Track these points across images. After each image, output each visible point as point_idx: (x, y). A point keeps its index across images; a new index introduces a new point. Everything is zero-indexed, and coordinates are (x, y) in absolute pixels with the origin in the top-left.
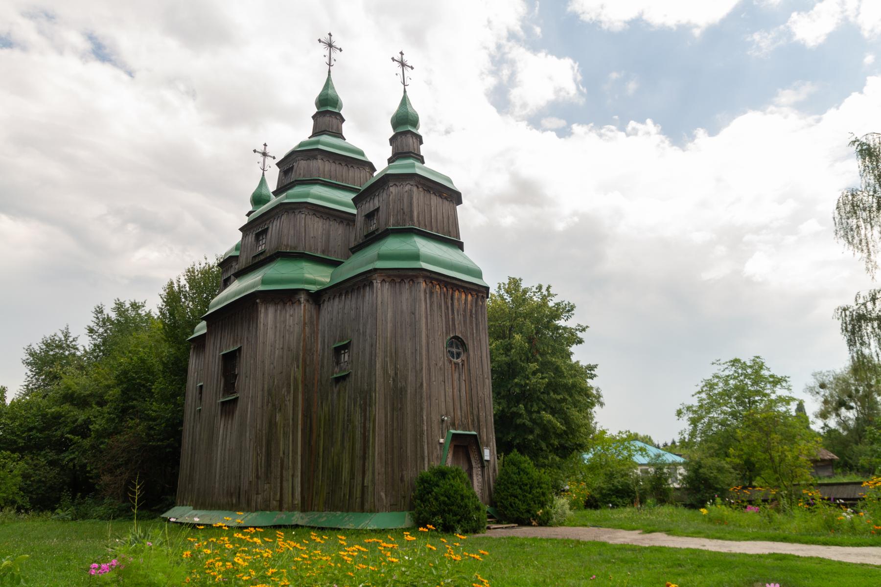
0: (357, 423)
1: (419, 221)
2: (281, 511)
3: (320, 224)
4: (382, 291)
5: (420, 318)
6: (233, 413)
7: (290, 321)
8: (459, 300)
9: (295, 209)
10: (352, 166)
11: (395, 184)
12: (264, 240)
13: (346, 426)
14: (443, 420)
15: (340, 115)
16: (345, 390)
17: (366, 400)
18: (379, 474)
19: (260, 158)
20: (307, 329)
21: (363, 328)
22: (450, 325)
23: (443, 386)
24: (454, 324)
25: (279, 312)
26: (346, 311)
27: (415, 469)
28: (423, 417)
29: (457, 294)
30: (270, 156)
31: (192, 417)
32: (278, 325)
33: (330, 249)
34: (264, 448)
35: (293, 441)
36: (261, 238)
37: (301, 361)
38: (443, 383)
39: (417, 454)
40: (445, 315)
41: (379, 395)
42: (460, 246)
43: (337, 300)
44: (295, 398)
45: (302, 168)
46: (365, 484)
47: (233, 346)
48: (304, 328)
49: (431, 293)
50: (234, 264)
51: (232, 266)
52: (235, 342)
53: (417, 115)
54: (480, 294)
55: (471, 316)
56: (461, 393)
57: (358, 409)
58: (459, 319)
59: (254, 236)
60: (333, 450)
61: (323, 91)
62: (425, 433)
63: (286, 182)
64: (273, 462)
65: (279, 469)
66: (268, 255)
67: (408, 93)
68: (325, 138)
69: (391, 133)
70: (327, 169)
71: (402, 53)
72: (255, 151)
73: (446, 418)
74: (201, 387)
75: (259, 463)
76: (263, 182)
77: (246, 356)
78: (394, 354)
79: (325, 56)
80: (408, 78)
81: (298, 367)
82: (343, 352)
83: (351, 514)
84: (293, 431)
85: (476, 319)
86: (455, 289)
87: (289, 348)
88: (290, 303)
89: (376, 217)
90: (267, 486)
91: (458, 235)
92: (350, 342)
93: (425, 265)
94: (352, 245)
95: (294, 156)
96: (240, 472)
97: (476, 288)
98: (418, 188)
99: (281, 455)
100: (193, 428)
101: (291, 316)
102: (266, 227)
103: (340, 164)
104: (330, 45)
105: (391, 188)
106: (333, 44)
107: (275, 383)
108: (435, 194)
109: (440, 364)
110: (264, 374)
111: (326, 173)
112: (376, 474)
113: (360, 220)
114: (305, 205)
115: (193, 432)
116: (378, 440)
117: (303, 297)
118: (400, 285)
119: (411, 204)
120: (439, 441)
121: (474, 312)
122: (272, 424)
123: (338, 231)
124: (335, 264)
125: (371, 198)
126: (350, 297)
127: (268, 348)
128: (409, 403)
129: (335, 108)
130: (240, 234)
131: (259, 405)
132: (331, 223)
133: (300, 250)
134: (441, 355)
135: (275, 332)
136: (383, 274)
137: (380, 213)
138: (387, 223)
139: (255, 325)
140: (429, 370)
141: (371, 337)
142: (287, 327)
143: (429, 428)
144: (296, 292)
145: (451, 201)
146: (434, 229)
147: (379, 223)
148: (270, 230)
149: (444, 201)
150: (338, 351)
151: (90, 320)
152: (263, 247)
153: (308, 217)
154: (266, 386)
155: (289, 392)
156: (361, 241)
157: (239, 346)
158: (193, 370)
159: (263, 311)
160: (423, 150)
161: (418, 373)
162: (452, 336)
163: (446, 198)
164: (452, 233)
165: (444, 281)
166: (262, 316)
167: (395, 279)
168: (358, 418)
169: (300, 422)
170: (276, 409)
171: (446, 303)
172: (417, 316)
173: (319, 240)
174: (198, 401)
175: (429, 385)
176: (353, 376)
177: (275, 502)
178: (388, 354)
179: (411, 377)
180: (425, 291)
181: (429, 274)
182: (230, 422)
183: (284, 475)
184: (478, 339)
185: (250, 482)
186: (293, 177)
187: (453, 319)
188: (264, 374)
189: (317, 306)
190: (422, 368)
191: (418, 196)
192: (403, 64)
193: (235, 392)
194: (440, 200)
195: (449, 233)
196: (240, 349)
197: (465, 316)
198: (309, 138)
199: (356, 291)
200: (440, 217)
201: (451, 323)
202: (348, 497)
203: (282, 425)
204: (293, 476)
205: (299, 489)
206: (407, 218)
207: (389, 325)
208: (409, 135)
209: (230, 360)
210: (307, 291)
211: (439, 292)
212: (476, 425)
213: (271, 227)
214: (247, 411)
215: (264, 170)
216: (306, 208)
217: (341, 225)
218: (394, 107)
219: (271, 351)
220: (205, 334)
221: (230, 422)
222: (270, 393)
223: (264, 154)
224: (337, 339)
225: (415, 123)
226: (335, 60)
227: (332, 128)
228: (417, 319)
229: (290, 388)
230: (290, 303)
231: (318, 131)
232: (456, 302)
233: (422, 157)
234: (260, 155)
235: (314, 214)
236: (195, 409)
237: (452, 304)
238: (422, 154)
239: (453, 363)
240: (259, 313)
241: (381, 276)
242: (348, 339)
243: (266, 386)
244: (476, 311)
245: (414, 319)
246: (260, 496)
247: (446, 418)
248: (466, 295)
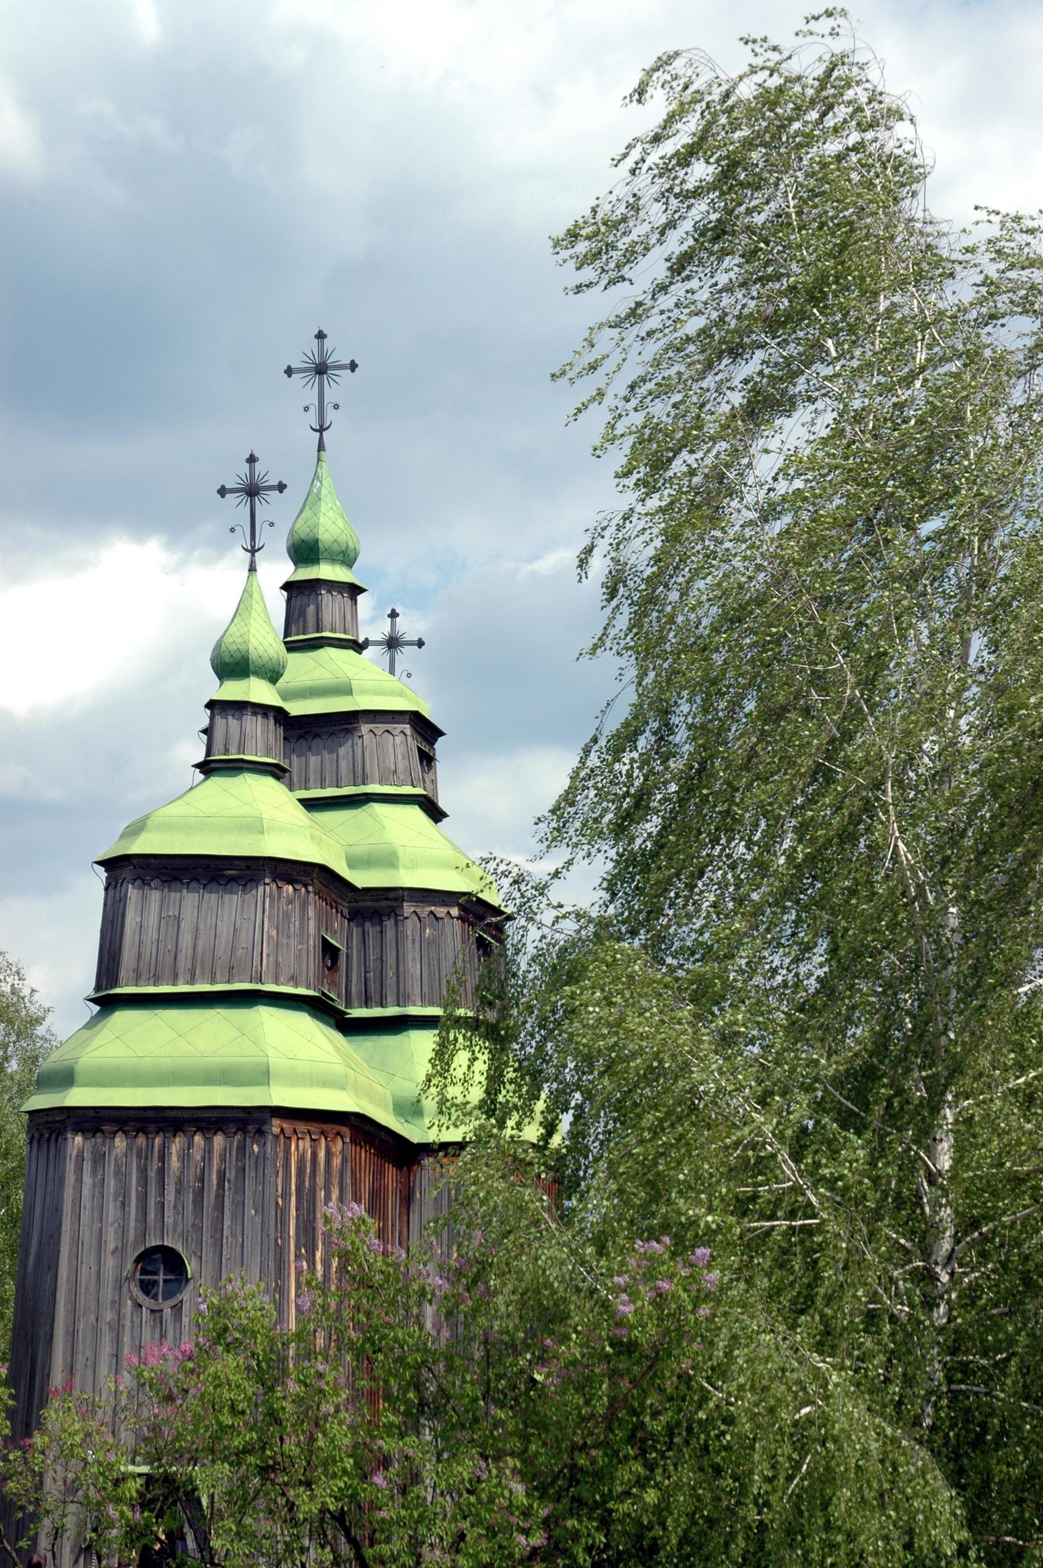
54: (250, 1128)
55: (221, 1186)
80: (266, 525)
104: (321, 369)
121: (231, 1174)
163: (233, 879)
180: (80, 1158)
192: (252, 491)
201: (152, 1216)
232: (174, 1162)
237: (162, 1172)
248: (206, 1139)
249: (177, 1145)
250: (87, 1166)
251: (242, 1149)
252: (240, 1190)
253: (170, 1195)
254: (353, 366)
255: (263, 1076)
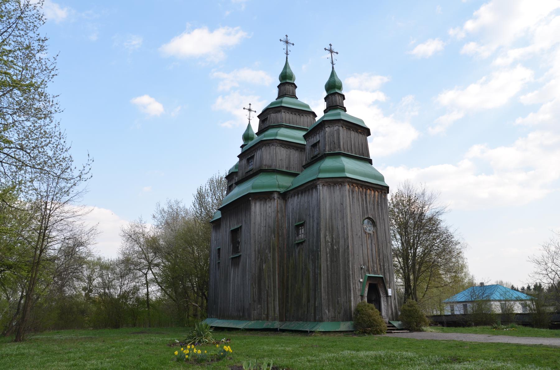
0: (310, 270)
2: (268, 320)
3: (285, 151)
4: (323, 191)
5: (346, 207)
6: (238, 264)
7: (269, 210)
8: (370, 195)
9: (270, 143)
10: (302, 115)
11: (329, 126)
12: (252, 163)
13: (304, 271)
14: (362, 268)
15: (294, 84)
16: (303, 250)
17: (315, 255)
18: (324, 299)
20: (279, 215)
21: (312, 213)
22: (365, 211)
23: (362, 248)
24: (367, 210)
25: (262, 205)
26: (302, 204)
27: (345, 297)
28: (349, 266)
29: (368, 191)
30: (253, 111)
31: (214, 267)
32: (262, 213)
33: (291, 166)
34: (257, 284)
35: (273, 280)
36: (250, 161)
37: (276, 233)
38: (361, 246)
39: (346, 288)
40: (362, 205)
41: (323, 253)
42: (370, 162)
43: (296, 197)
44: (274, 255)
45: (273, 118)
46: (316, 306)
47: (237, 225)
48: (277, 214)
49: (353, 191)
50: (234, 177)
51: (233, 178)
52: (238, 223)
53: (341, 82)
54: (383, 191)
55: (378, 205)
56: (373, 251)
57: (311, 262)
59: (246, 160)
60: (296, 286)
61: (283, 70)
62: (351, 276)
63: (263, 127)
64: (262, 292)
65: (266, 296)
66: (255, 171)
67: (335, 69)
68: (286, 99)
69: (325, 94)
70: (287, 118)
71: (330, 45)
72: (244, 108)
73: (364, 267)
74: (219, 249)
75: (255, 293)
76: (249, 126)
77: (245, 231)
78: (331, 229)
79: (284, 49)
81: (275, 237)
82: (300, 228)
83: (309, 322)
84: (273, 275)
85: (381, 207)
86: (367, 188)
87: (269, 226)
88: (269, 199)
89: (318, 147)
90: (259, 306)
91: (368, 155)
92: (304, 222)
94: (304, 164)
95: (268, 111)
96: (244, 298)
97: (381, 187)
98: (343, 127)
99: (267, 288)
100: (215, 274)
101: (270, 207)
102: (253, 155)
103: (295, 114)
104: (287, 42)
105: (326, 129)
106: (289, 41)
107: (262, 247)
108: (354, 131)
109: (359, 234)
110: (255, 242)
111: (287, 120)
112: (323, 299)
113: (308, 148)
114: (275, 141)
115: (215, 276)
116: (323, 280)
117: (276, 196)
118: (333, 187)
120: (359, 280)
121: (379, 202)
122: (261, 270)
123: (295, 155)
124: (295, 175)
125: (314, 135)
126: (304, 195)
127: (257, 227)
128: (341, 258)
129: (291, 80)
130: (238, 159)
131: (253, 259)
132: (291, 150)
133: (273, 168)
134: (360, 229)
135: (261, 217)
136: (323, 181)
137: (320, 144)
138: (325, 150)
139: (249, 213)
140: (353, 238)
141: (317, 219)
142: (268, 214)
143: (353, 273)
144: (272, 193)
145: (364, 134)
146: (354, 152)
147: (319, 150)
148: (255, 156)
149: (360, 134)
150: (298, 227)
152: (252, 167)
153: (278, 148)
154: (257, 248)
155: (270, 252)
156: (309, 161)
157: (240, 225)
158: (214, 240)
159: (253, 204)
160: (346, 103)
161: (346, 240)
162: (366, 217)
163: (360, 133)
164: (365, 154)
165: (360, 184)
166: (253, 207)
167: (330, 184)
168: (310, 267)
169: (277, 269)
170: (263, 262)
171: (362, 197)
172: (344, 206)
173: (284, 161)
174: (217, 258)
175: (353, 247)
176: (307, 243)
177: (264, 315)
178: (328, 229)
179: (342, 242)
181: (351, 180)
182: (237, 269)
183: (269, 300)
184: (383, 219)
185: (250, 304)
186: (267, 124)
187: (367, 207)
188: (255, 242)
189: (285, 201)
190: (348, 237)
191: (343, 132)
193: (239, 252)
194: (357, 134)
195: (363, 155)
196: (241, 227)
197: (374, 205)
198: (276, 99)
199: (307, 192)
200: (357, 145)
202: (306, 313)
203: (267, 271)
204: (274, 300)
205: (278, 308)
206: (337, 147)
207: (328, 212)
208: (337, 95)
209: (235, 233)
210: (279, 192)
211: (357, 191)
212: (382, 271)
213: (256, 154)
214: (246, 263)
215: (249, 119)
216: (276, 142)
217: (297, 151)
218: (326, 78)
219: (259, 228)
220: (220, 218)
221: (237, 269)
222: (259, 253)
223: (250, 110)
224: (297, 221)
225: (340, 88)
226: (290, 51)
227: (290, 93)
228: (344, 207)
229: (270, 249)
230: (269, 199)
231: (281, 95)
232: (368, 196)
233: (345, 108)
234: (247, 111)
235: (281, 146)
236: (216, 262)
238: (344, 106)
239: (367, 233)
240: (251, 206)
241: (322, 182)
242: (303, 220)
243: (257, 248)
245: (342, 208)
246: (255, 312)
247: (364, 267)
250: (351, 193)
251: (381, 196)
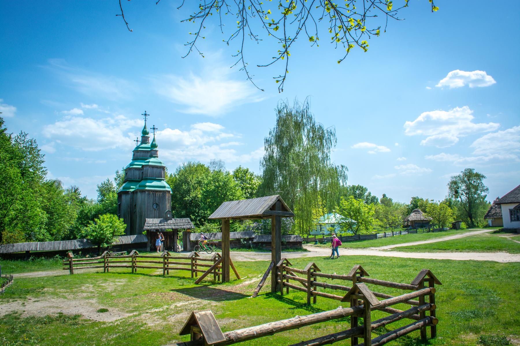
1: (150, 176)
19: (136, 142)
44: (128, 215)
58: (157, 199)
85: (163, 198)
93: (147, 188)
104: (146, 115)
119: (148, 172)
151: (115, 176)
171: (154, 196)
187: (155, 199)
232: (157, 195)
244: (163, 196)
249: (157, 193)
251: (163, 194)
252: (163, 198)
253: (156, 198)
254: (149, 115)
255: (164, 187)
